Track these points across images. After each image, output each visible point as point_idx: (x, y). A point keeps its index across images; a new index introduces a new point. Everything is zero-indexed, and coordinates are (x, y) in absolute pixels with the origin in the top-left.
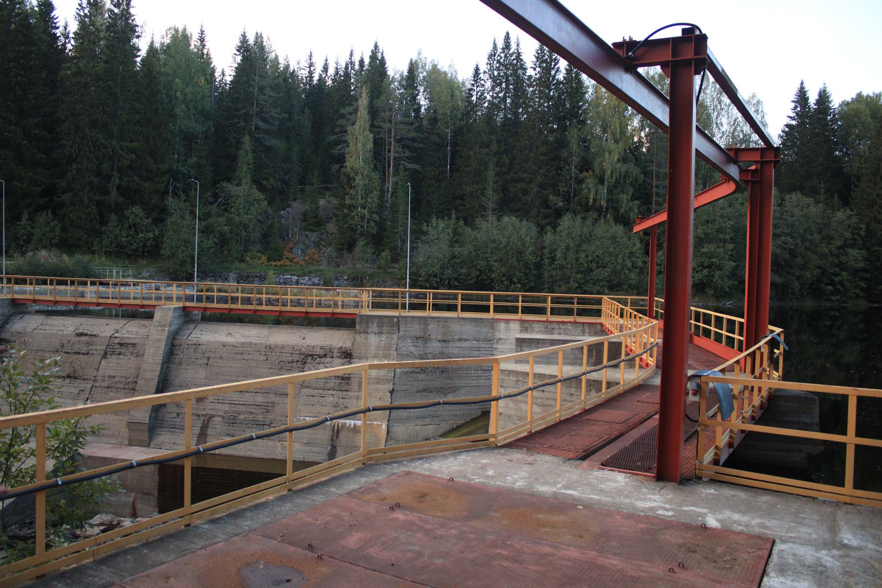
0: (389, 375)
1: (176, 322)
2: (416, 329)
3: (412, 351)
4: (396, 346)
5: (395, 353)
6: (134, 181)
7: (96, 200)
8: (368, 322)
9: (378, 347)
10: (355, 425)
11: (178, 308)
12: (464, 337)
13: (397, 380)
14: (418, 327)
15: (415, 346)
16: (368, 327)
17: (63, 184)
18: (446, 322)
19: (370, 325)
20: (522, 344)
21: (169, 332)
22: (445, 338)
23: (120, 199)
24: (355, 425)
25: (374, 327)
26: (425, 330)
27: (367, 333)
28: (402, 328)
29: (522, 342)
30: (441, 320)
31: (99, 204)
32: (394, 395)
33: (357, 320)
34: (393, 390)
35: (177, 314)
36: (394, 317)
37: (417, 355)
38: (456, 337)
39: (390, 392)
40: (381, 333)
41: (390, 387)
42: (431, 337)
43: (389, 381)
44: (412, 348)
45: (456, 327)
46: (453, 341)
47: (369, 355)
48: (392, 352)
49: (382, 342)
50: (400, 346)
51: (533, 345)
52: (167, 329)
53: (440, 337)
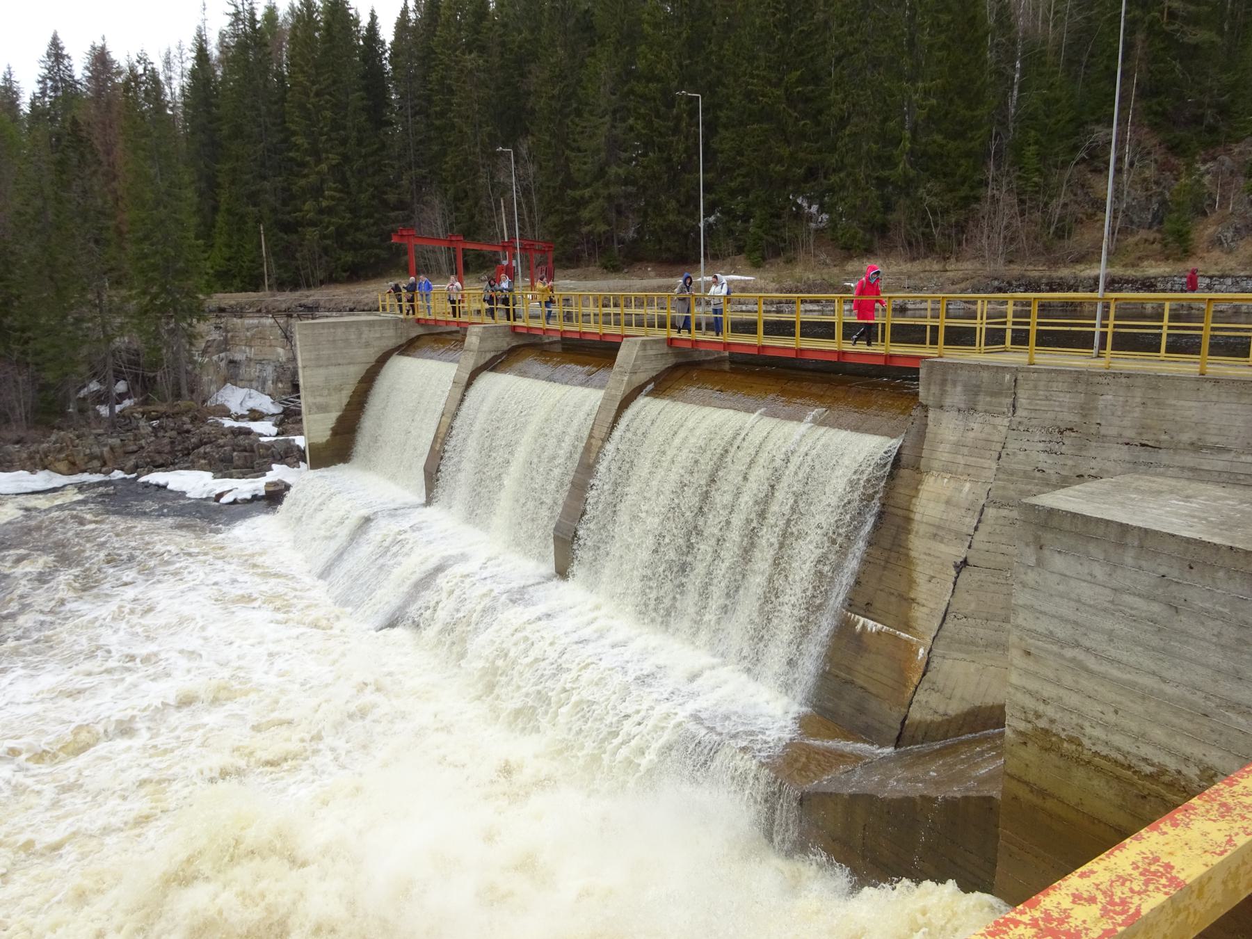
0: (968, 520)
1: (649, 366)
2: (1063, 406)
3: (1040, 466)
4: (998, 447)
5: (994, 466)
6: (934, 142)
7: (877, 178)
8: (944, 382)
9: (958, 445)
10: (864, 626)
11: (657, 342)
12: (1211, 440)
13: (979, 536)
14: (1066, 398)
15: (1050, 452)
16: (943, 392)
17: (833, 159)
18: (1155, 388)
19: (949, 388)
20: (1048, 537)
21: (629, 382)
22: (1148, 438)
23: (912, 173)
24: (864, 626)
25: (956, 396)
26: (1086, 411)
27: (941, 407)
28: (1023, 401)
29: (1045, 526)
30: (1139, 381)
31: (882, 183)
32: (964, 574)
33: (922, 373)
34: (965, 562)
35: (651, 352)
36: (1004, 369)
37: (1054, 478)
38: (1186, 437)
39: (956, 566)
40: (972, 409)
41: (957, 552)
42: (1103, 431)
43: (959, 536)
44: (1043, 456)
45: (1188, 408)
46: (1175, 448)
47: (936, 464)
48: (987, 463)
49: (971, 434)
50: (1012, 446)
51: (1093, 549)
52: (626, 378)
53: (1130, 434)
